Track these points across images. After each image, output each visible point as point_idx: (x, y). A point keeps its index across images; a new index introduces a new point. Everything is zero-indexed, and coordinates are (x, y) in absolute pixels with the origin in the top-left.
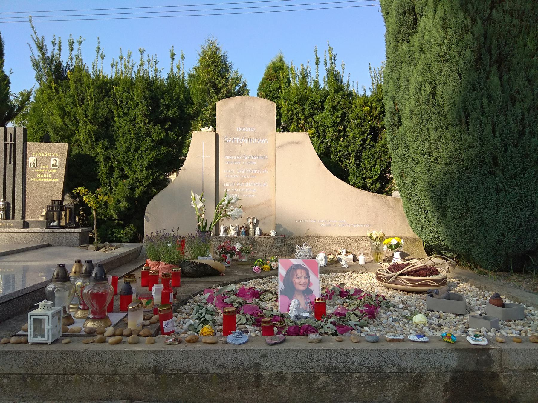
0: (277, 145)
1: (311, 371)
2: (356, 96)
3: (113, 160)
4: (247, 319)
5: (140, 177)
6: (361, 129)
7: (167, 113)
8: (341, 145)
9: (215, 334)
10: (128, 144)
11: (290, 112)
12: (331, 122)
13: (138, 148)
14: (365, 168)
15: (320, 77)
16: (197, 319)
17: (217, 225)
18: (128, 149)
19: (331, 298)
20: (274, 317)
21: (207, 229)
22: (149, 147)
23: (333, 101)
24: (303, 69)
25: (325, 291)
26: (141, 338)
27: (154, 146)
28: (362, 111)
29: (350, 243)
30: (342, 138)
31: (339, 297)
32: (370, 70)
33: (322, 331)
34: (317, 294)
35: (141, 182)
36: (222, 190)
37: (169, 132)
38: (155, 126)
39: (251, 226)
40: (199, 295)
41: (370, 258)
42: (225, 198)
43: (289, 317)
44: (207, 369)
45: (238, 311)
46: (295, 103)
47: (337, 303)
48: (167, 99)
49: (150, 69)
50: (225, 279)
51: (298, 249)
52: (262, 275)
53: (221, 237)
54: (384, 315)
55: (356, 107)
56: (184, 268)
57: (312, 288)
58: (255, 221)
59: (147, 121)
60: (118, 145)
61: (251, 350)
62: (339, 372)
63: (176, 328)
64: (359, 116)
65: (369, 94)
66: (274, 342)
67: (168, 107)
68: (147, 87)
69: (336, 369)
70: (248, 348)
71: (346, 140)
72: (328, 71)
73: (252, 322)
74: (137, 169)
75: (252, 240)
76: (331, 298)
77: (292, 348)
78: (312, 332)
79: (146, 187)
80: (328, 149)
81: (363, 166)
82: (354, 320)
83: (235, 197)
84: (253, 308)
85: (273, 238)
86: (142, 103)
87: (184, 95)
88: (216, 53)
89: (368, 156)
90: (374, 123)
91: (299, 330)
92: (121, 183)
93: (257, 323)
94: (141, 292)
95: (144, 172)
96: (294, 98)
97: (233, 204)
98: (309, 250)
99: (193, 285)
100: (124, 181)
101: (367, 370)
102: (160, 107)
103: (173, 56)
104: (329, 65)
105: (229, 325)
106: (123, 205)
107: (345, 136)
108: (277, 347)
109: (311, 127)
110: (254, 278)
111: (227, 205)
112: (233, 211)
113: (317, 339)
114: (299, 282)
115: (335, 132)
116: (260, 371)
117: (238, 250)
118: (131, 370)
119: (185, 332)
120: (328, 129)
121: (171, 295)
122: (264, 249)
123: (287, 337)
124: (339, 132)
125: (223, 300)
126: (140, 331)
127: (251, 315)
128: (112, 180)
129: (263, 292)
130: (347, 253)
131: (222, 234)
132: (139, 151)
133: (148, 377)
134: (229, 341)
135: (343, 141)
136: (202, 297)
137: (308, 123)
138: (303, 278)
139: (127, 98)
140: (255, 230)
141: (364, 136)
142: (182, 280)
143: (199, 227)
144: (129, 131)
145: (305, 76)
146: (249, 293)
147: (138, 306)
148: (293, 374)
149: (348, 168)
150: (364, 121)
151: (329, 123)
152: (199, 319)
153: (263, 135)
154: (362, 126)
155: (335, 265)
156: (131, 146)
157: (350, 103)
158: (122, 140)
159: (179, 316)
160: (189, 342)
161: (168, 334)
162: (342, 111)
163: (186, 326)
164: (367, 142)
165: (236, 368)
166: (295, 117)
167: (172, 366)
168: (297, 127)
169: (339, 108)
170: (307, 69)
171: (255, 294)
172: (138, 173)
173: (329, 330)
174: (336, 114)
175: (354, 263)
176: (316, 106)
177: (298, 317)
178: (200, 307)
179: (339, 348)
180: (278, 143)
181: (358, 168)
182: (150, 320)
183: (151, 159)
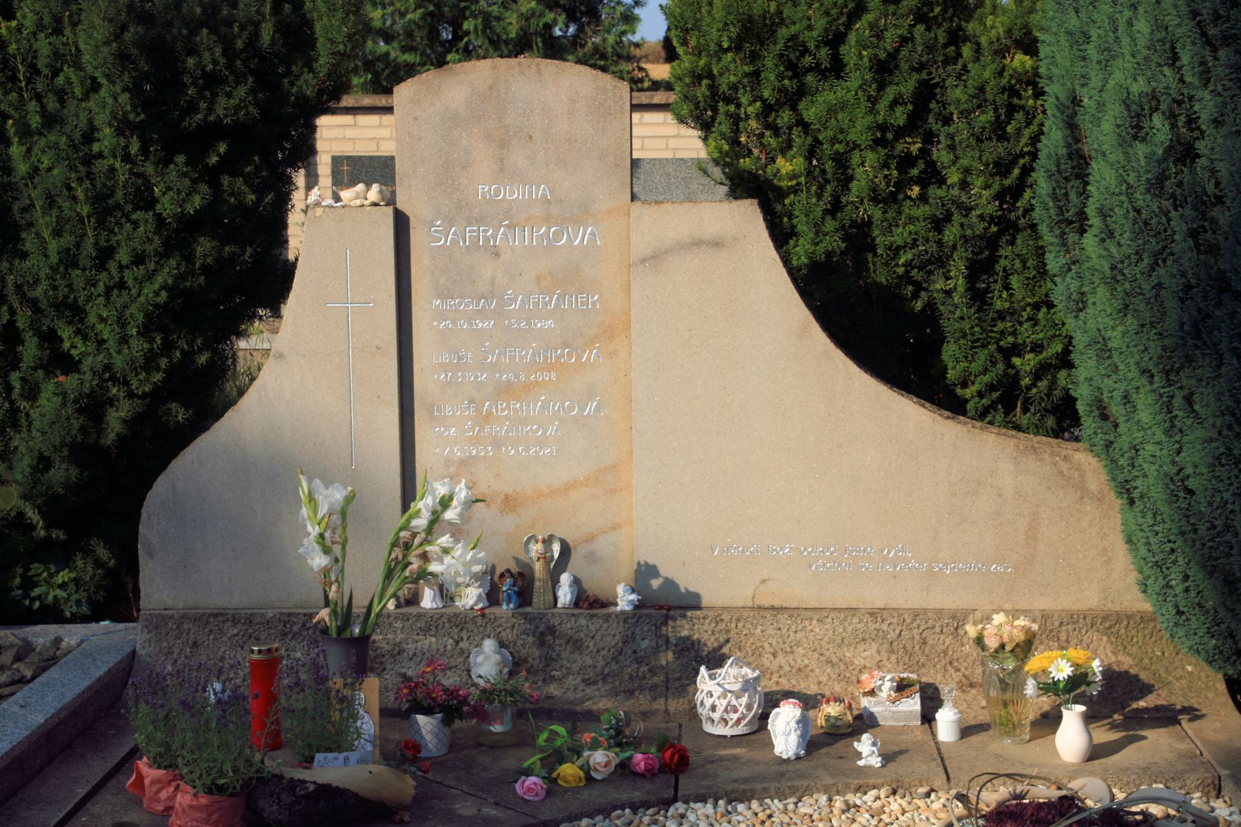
0: (637, 253)
3: (15, 301)
5: (119, 362)
7: (210, 110)
8: (911, 220)
10: (68, 240)
13: (105, 255)
14: (1012, 312)
18: (69, 260)
22: (149, 248)
27: (165, 243)
37: (226, 180)
38: (167, 161)
39: (538, 567)
48: (210, 55)
58: (556, 548)
59: (134, 148)
60: (29, 242)
67: (212, 82)
74: (106, 332)
75: (542, 628)
80: (859, 238)
85: (624, 617)
92: (48, 388)
95: (134, 343)
100: (62, 378)
106: (61, 473)
107: (933, 176)
109: (785, 149)
111: (430, 530)
115: (886, 165)
122: (589, 661)
124: (907, 161)
128: (15, 377)
130: (902, 687)
132: (113, 266)
135: (923, 198)
137: (776, 131)
139: (56, 55)
140: (555, 582)
141: (1007, 182)
144: (69, 188)
150: (1010, 116)
151: (860, 128)
153: (581, 214)
154: (1003, 137)
156: (78, 245)
158: (44, 223)
162: (915, 76)
169: (904, 66)
172: (112, 345)
174: (890, 93)
183: (157, 294)
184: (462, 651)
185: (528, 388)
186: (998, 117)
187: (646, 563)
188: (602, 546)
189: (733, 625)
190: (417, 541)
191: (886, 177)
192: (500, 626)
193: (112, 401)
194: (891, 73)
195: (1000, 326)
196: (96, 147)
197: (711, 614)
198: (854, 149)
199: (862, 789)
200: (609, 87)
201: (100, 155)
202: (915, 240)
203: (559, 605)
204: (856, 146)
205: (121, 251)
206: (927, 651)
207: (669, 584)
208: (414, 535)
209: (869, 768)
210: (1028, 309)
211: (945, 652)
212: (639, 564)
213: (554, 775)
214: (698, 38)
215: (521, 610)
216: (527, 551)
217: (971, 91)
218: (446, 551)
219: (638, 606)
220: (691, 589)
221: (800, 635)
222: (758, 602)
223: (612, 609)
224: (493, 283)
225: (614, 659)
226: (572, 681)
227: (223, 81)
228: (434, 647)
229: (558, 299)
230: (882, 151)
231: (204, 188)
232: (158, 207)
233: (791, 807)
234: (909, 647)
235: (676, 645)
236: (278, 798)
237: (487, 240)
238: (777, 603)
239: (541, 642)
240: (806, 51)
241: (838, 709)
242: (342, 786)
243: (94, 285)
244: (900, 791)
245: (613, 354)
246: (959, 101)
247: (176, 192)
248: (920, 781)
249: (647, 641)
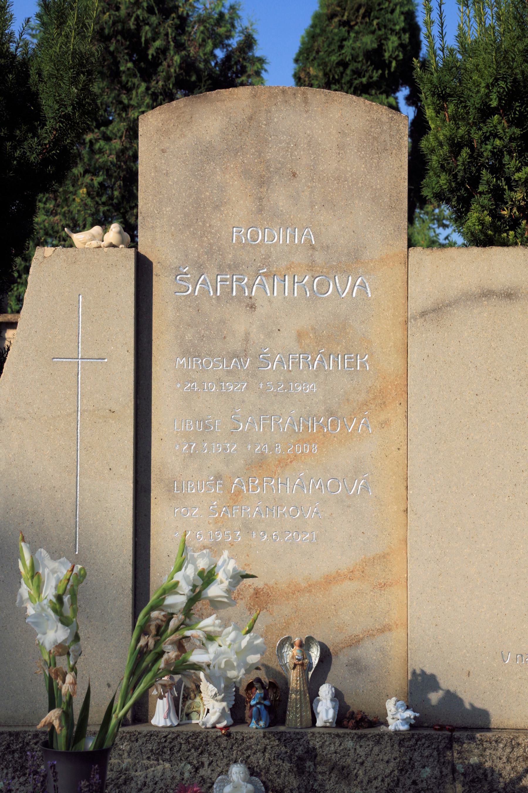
0: (416, 304)
11: (465, 152)
39: (294, 678)
42: (179, 577)
46: (486, 112)
58: (315, 654)
75: (300, 751)
83: (227, 566)
97: (215, 605)
111: (188, 610)
131: (161, 716)
140: (314, 695)
153: (351, 261)
168: (495, 215)
184: (203, 780)
185: (284, 462)
187: (423, 673)
188: (367, 652)
190: (173, 623)
192: (248, 748)
197: (504, 735)
200: (385, 119)
203: (319, 723)
207: (451, 698)
208: (170, 617)
212: (414, 673)
214: (456, 105)
215: (272, 729)
216: (280, 656)
218: (211, 637)
219: (415, 726)
220: (478, 705)
223: (383, 728)
224: (247, 339)
228: (168, 774)
229: (321, 360)
235: (464, 775)
237: (241, 290)
239: (300, 771)
245: (385, 424)
249: (428, 769)
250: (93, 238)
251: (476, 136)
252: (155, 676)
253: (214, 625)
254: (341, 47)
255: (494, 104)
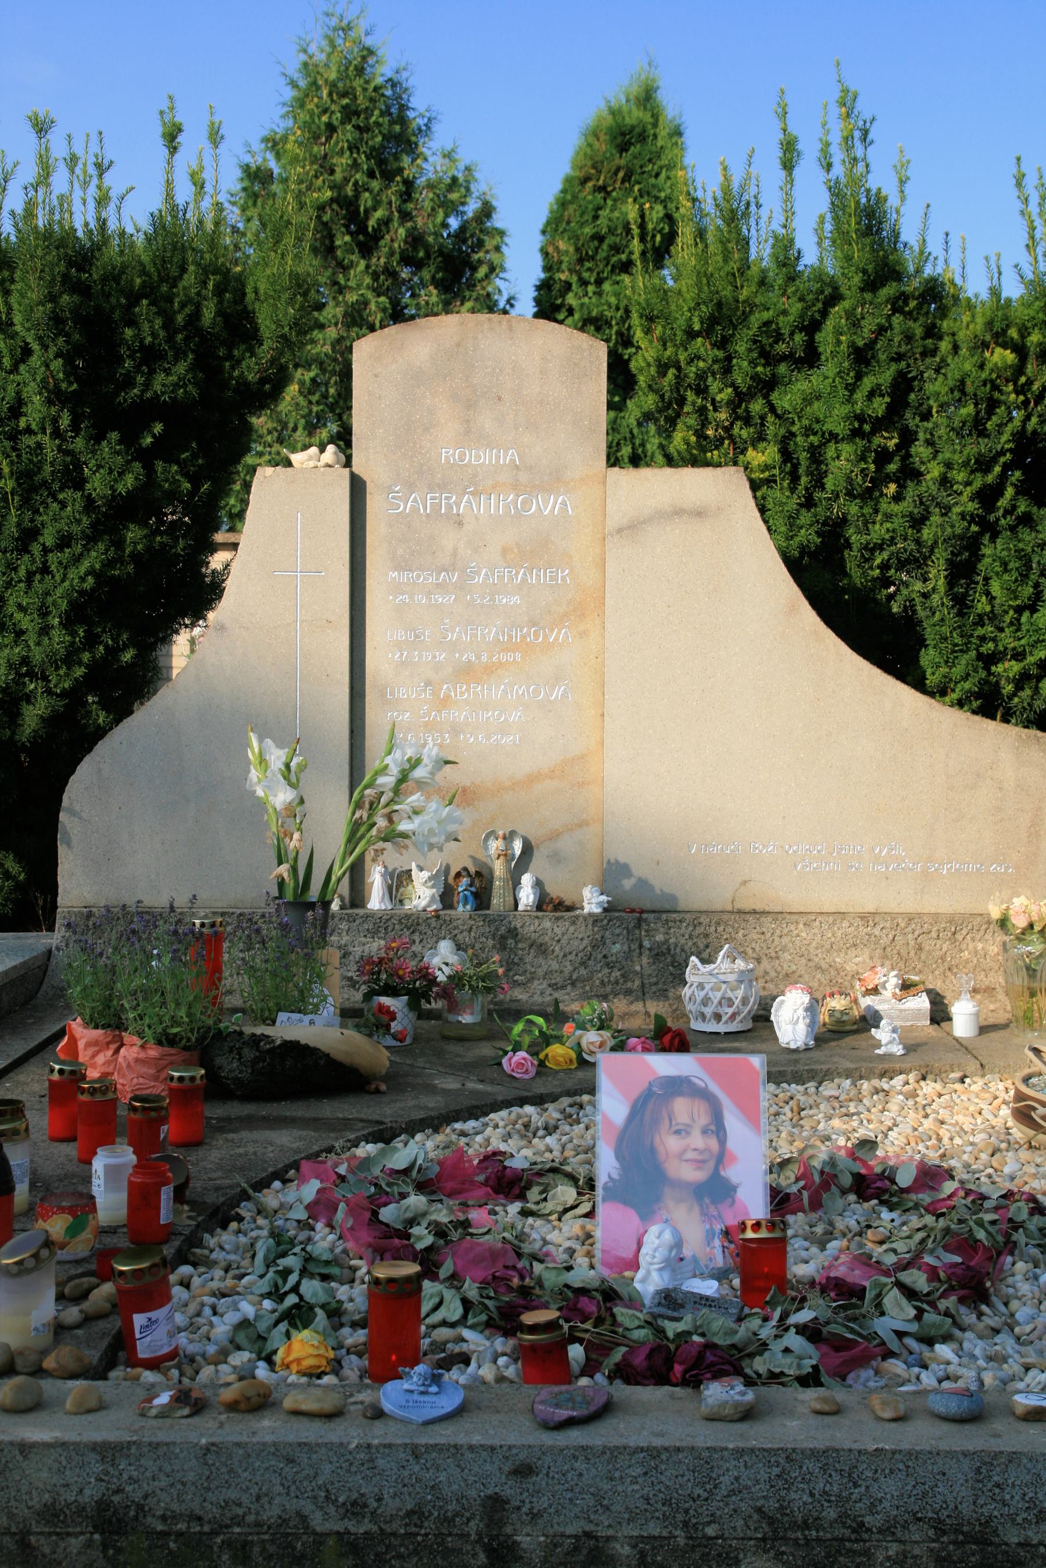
1: (710, 1531)
2: (956, 299)
4: (466, 1303)
5: (38, 655)
6: (973, 448)
7: (147, 385)
8: (888, 517)
9: (336, 1366)
11: (671, 372)
12: (847, 418)
13: (28, 535)
14: (993, 617)
15: (798, 221)
16: (268, 1295)
17: (357, 873)
19: (816, 1204)
20: (574, 1298)
21: (314, 893)
22: (76, 529)
23: (855, 324)
24: (727, 190)
25: (790, 1174)
26: (48, 1386)
27: (93, 525)
28: (982, 366)
29: (916, 943)
30: (893, 487)
31: (852, 1197)
32: (1019, 184)
33: (760, 1365)
34: (754, 1204)
35: (45, 679)
36: (377, 718)
37: (159, 466)
38: (99, 438)
39: (499, 868)
40: (277, 1184)
41: (1001, 1008)
42: (388, 760)
43: (634, 1302)
44: (303, 1518)
45: (429, 1263)
46: (691, 334)
47: (840, 1224)
48: (148, 326)
49: (78, 193)
50: (388, 1110)
51: (696, 971)
52: (540, 1088)
53: (370, 916)
54: (1025, 1288)
55: (956, 348)
56: (219, 1061)
57: (732, 1173)
58: (518, 846)
59: (65, 421)
61: (471, 1448)
62: (818, 1540)
63: (182, 1339)
64: (970, 389)
65: (1013, 290)
66: (564, 1414)
68: (66, 277)
69: (805, 1525)
70: (462, 1439)
71: (911, 491)
72: (835, 191)
73: (484, 1317)
74: (25, 622)
75: (503, 930)
76: (816, 1204)
77: (633, 1441)
78: (717, 1376)
79: (64, 694)
80: (834, 532)
81: (982, 605)
82: (897, 1314)
83: (430, 752)
84: (494, 1255)
85: (595, 919)
86: (45, 347)
87: (220, 302)
88: (360, 71)
89: (1005, 564)
90: (1034, 420)
91: (670, 1360)
93: (504, 1322)
94: (47, 1169)
96: (685, 313)
97: (420, 784)
98: (746, 978)
99: (256, 1135)
101: (931, 1533)
102: (120, 360)
103: (172, 136)
104: (838, 170)
105: (393, 1337)
107: (910, 474)
108: (575, 1436)
109: (760, 438)
110: (507, 1104)
111: (397, 790)
112: (422, 815)
113: (737, 1404)
114: (681, 1150)
115: (863, 458)
116: (508, 1530)
117: (441, 978)
118: (11, 1516)
119: (223, 1356)
120: (832, 446)
121: (166, 1194)
122: (555, 966)
123: (621, 1390)
124: (883, 457)
125: (375, 1214)
126: (44, 1353)
127: (485, 1284)
129: (540, 1174)
130: (906, 987)
131: (376, 901)
132: (36, 549)
133: (75, 1544)
134: (387, 1406)
135: (898, 498)
136: (291, 1194)
137: (747, 421)
138: (696, 1133)
140: (516, 883)
141: (990, 478)
142: (215, 1111)
143: (281, 884)
145: (736, 214)
146: (481, 1178)
147: (36, 1256)
148: (635, 1542)
149: (921, 613)
150: (990, 412)
151: (837, 419)
152: (276, 1294)
153: (552, 481)
154: (983, 433)
155: (849, 1040)
157: (932, 332)
159: (196, 1281)
160: (232, 1407)
161: (153, 1364)
162: (894, 367)
163: (222, 1329)
164: (1003, 503)
165: (416, 1514)
166: (690, 396)
167: (165, 1502)
168: (700, 435)
169: (882, 357)
170: (743, 188)
171: (509, 1184)
172: (31, 638)
173: (789, 1360)
174: (868, 383)
175: (932, 1031)
176: (782, 348)
177: (671, 1300)
178: (282, 1244)
179: (820, 1445)
180: (616, 517)
181: (960, 614)
182: (86, 1305)
183: (83, 579)
185: (490, 670)
186: (978, 413)
187: (617, 861)
189: (713, 929)
190: (384, 800)
191: (863, 470)
192: (455, 928)
193: (29, 698)
194: (868, 363)
195: (980, 631)
196: (22, 423)
197: (688, 916)
198: (829, 441)
199: (887, 1074)
200: (585, 346)
201: (28, 430)
202: (893, 538)
203: (521, 908)
204: (834, 437)
205: (46, 531)
206: (923, 956)
207: (642, 883)
209: (888, 1057)
210: (1011, 612)
211: (943, 958)
212: (609, 862)
213: (542, 1056)
214: (664, 327)
216: (486, 848)
217: (951, 383)
218: (416, 812)
219: (608, 909)
220: (666, 890)
221: (785, 940)
222: (738, 905)
223: (578, 912)
224: (455, 553)
225: (583, 964)
226: (537, 986)
227: (161, 356)
229: (525, 574)
230: (860, 443)
231: (137, 466)
232: (88, 486)
233: (813, 1090)
234: (904, 953)
235: (650, 949)
236: (239, 1054)
237: (449, 507)
238: (759, 907)
240: (779, 337)
241: (843, 1002)
242: (312, 1045)
243: (15, 569)
244: (930, 1077)
245: (584, 634)
246: (938, 394)
247: (109, 471)
248: (952, 1066)
249: (618, 945)
250: (310, 458)
251: (682, 357)
252: (368, 842)
253: (418, 800)
254: (596, 217)
255: (697, 327)
